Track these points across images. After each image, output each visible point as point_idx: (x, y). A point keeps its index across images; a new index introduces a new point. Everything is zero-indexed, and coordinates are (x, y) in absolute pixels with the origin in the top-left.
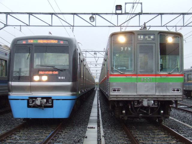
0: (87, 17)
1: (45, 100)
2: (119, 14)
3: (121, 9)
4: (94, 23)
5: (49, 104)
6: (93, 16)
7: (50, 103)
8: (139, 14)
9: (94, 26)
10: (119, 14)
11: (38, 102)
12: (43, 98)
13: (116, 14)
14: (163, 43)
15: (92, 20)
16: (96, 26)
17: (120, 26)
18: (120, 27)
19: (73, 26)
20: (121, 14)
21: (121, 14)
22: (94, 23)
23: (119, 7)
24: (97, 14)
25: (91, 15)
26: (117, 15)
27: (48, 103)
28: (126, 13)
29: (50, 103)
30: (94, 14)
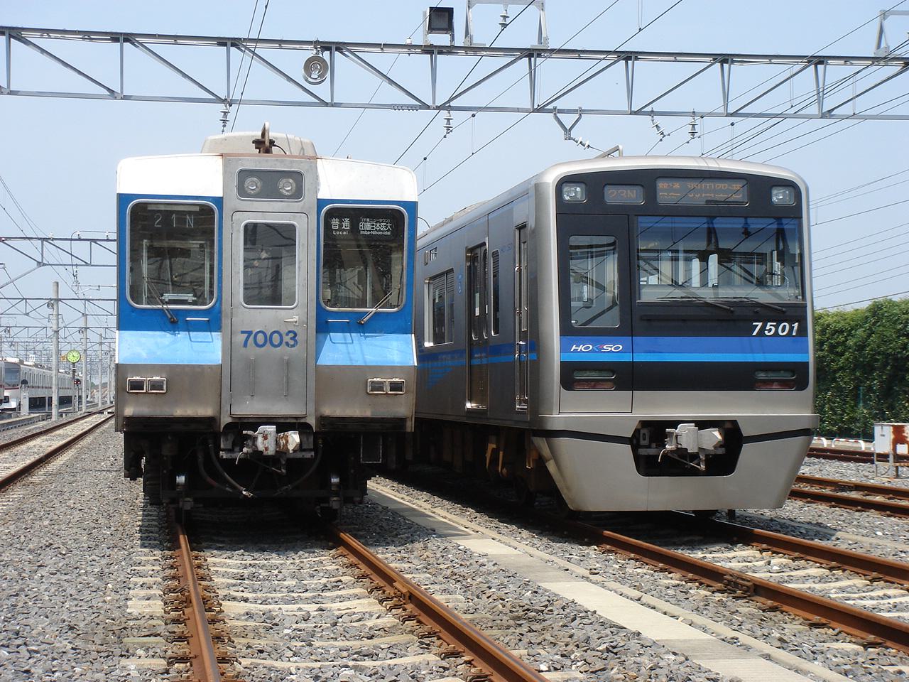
0: (293, 62)
2: (442, 50)
3: (449, 28)
4: (323, 91)
6: (324, 53)
8: (530, 53)
9: (326, 105)
10: (442, 50)
13: (429, 50)
14: (541, 183)
15: (315, 75)
16: (333, 105)
20: (449, 53)
21: (450, 50)
22: (323, 91)
23: (441, 18)
24: (340, 47)
25: (311, 53)
26: (429, 56)
28: (471, 49)
30: (326, 46)
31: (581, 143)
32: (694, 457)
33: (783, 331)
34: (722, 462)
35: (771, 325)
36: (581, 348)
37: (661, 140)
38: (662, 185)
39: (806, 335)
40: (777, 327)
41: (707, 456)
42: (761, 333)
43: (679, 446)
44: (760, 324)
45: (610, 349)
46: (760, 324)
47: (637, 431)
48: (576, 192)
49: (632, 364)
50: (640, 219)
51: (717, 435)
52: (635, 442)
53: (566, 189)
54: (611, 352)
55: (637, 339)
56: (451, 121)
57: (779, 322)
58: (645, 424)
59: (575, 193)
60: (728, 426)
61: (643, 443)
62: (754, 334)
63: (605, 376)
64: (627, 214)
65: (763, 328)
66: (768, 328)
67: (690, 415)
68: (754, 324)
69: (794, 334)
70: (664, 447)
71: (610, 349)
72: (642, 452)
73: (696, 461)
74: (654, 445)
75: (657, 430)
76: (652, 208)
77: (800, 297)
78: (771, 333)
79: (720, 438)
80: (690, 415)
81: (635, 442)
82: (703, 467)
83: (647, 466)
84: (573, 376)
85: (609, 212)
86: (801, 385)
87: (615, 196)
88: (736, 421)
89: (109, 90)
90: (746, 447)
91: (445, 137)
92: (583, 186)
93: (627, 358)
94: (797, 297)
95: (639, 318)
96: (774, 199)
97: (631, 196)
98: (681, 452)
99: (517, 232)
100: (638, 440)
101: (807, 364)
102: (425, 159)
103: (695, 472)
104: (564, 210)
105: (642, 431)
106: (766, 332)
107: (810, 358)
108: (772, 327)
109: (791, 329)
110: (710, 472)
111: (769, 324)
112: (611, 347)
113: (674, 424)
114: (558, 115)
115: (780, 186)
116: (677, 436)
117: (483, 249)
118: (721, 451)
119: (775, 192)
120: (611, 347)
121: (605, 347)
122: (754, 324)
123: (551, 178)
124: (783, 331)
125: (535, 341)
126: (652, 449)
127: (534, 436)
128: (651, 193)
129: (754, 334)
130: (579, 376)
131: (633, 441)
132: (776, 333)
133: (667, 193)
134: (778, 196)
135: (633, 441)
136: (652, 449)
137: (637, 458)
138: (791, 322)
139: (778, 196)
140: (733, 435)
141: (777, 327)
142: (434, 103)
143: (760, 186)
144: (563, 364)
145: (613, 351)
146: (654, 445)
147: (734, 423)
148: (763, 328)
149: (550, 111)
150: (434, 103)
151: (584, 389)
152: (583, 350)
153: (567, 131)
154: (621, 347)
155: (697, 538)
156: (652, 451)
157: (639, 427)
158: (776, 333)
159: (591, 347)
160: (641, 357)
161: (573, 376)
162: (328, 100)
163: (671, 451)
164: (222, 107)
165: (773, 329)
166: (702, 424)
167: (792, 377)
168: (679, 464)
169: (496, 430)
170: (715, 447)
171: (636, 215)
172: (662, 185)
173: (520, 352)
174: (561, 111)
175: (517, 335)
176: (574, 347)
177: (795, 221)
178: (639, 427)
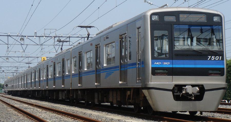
32: (191, 95)
33: (217, 59)
34: (199, 97)
36: (158, 63)
37: (175, 2)
38: (181, 16)
41: (194, 95)
42: (210, 59)
43: (187, 92)
44: (210, 57)
46: (210, 57)
47: (174, 88)
48: (156, 18)
49: (173, 68)
50: (175, 26)
51: (197, 88)
52: (173, 91)
53: (153, 17)
54: (166, 64)
55: (174, 61)
57: (216, 56)
58: (176, 86)
59: (155, 18)
60: (201, 86)
61: (175, 91)
64: (171, 24)
65: (211, 58)
66: (212, 58)
67: (189, 83)
69: (220, 59)
70: (182, 92)
72: (175, 94)
73: (191, 97)
74: (179, 92)
75: (180, 87)
76: (178, 22)
77: (222, 49)
78: (213, 59)
79: (198, 89)
80: (189, 83)
81: (173, 91)
82: (193, 98)
83: (177, 98)
84: (155, 71)
85: (166, 24)
86: (222, 74)
87: (167, 19)
88: (203, 85)
90: (206, 93)
92: (158, 16)
93: (171, 66)
94: (221, 49)
95: (175, 55)
96: (214, 20)
97: (172, 19)
98: (187, 93)
99: (137, 30)
100: (174, 91)
101: (224, 68)
102: (99, 8)
103: (191, 100)
104: (152, 23)
105: (175, 88)
106: (212, 59)
107: (225, 67)
109: (219, 58)
110: (195, 100)
111: (213, 56)
113: (185, 86)
115: (215, 16)
116: (186, 89)
117: (125, 35)
118: (198, 94)
119: (214, 18)
123: (149, 14)
124: (217, 59)
125: (143, 62)
126: (179, 93)
127: (143, 89)
128: (178, 18)
131: (173, 91)
132: (215, 59)
133: (183, 18)
134: (215, 19)
135: (173, 91)
136: (179, 93)
137: (174, 95)
138: (219, 56)
139: (215, 19)
140: (202, 89)
141: (215, 57)
143: (210, 16)
144: (152, 68)
145: (167, 64)
146: (179, 92)
147: (202, 85)
148: (211, 58)
151: (158, 75)
152: (158, 64)
154: (169, 63)
156: (178, 94)
157: (175, 87)
160: (174, 66)
161: (155, 71)
163: (184, 94)
165: (214, 58)
166: (193, 86)
167: (219, 72)
168: (186, 98)
169: (129, 89)
170: (197, 92)
172: (181, 16)
173: (138, 65)
175: (137, 60)
176: (155, 63)
177: (220, 26)
178: (175, 87)
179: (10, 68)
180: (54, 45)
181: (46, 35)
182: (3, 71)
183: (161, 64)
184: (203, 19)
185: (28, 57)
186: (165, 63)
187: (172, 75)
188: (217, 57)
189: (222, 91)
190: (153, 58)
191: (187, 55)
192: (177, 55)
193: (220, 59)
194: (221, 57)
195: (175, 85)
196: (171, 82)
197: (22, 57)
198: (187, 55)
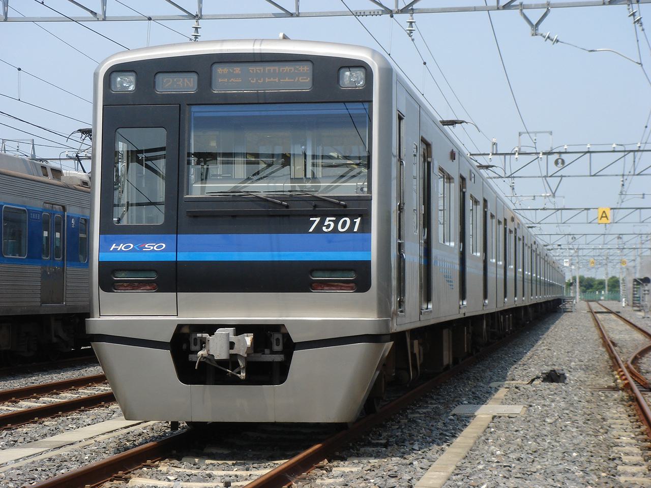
1: (248, 339)
5: (273, 353)
7: (276, 348)
9: (292, 15)
11: (217, 347)
12: (241, 329)
17: (407, 10)
18: (407, 17)
19: (197, 17)
27: (267, 351)
29: (276, 348)
31: (548, 37)
33: (343, 227)
35: (329, 221)
36: (122, 247)
39: (369, 231)
40: (336, 223)
42: (318, 230)
44: (318, 220)
45: (152, 248)
46: (318, 220)
50: (194, 109)
54: (153, 251)
56: (413, 24)
57: (339, 216)
59: (127, 83)
62: (311, 230)
63: (153, 276)
65: (321, 223)
68: (311, 219)
69: (356, 230)
71: (152, 248)
73: (237, 370)
76: (205, 97)
77: (366, 189)
78: (330, 229)
82: (243, 375)
86: (362, 285)
87: (168, 85)
89: (92, 12)
90: (297, 354)
91: (413, 40)
93: (171, 257)
94: (362, 189)
97: (187, 84)
101: (368, 263)
106: (324, 229)
108: (331, 223)
110: (250, 381)
111: (328, 219)
112: (153, 246)
113: (211, 329)
114: (524, 11)
120: (153, 246)
121: (146, 246)
122: (311, 219)
124: (343, 227)
128: (206, 82)
129: (311, 230)
130: (121, 277)
132: (335, 230)
133: (226, 81)
138: (352, 216)
141: (336, 223)
142: (397, 6)
143: (327, 70)
144: (101, 264)
145: (155, 249)
148: (321, 223)
149: (516, 7)
150: (397, 6)
152: (123, 250)
153: (535, 27)
154: (164, 245)
155: (226, 452)
158: (335, 230)
159: (132, 246)
160: (183, 257)
161: (114, 277)
162: (292, 10)
164: (193, 23)
165: (332, 225)
171: (188, 105)
172: (220, 70)
174: (529, 7)
176: (113, 246)
177: (366, 105)
179: (554, 238)
180: (545, 177)
181: (523, 150)
182: (559, 245)
183: (133, 250)
184: (301, 81)
185: (560, 209)
186: (149, 247)
187: (176, 290)
188: (345, 222)
189: (361, 346)
190: (108, 228)
191: (234, 216)
192: (195, 217)
193: (356, 230)
194: (358, 221)
195: (178, 325)
196: (160, 313)
197: (544, 209)
198: (234, 216)
